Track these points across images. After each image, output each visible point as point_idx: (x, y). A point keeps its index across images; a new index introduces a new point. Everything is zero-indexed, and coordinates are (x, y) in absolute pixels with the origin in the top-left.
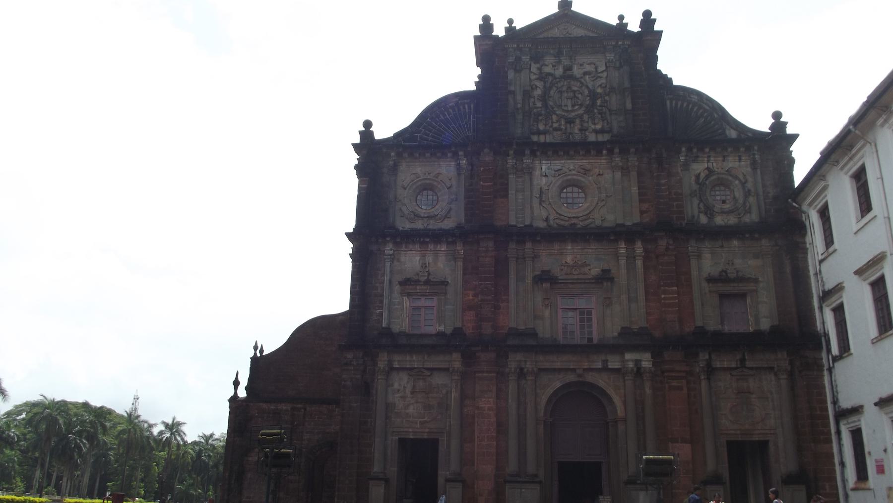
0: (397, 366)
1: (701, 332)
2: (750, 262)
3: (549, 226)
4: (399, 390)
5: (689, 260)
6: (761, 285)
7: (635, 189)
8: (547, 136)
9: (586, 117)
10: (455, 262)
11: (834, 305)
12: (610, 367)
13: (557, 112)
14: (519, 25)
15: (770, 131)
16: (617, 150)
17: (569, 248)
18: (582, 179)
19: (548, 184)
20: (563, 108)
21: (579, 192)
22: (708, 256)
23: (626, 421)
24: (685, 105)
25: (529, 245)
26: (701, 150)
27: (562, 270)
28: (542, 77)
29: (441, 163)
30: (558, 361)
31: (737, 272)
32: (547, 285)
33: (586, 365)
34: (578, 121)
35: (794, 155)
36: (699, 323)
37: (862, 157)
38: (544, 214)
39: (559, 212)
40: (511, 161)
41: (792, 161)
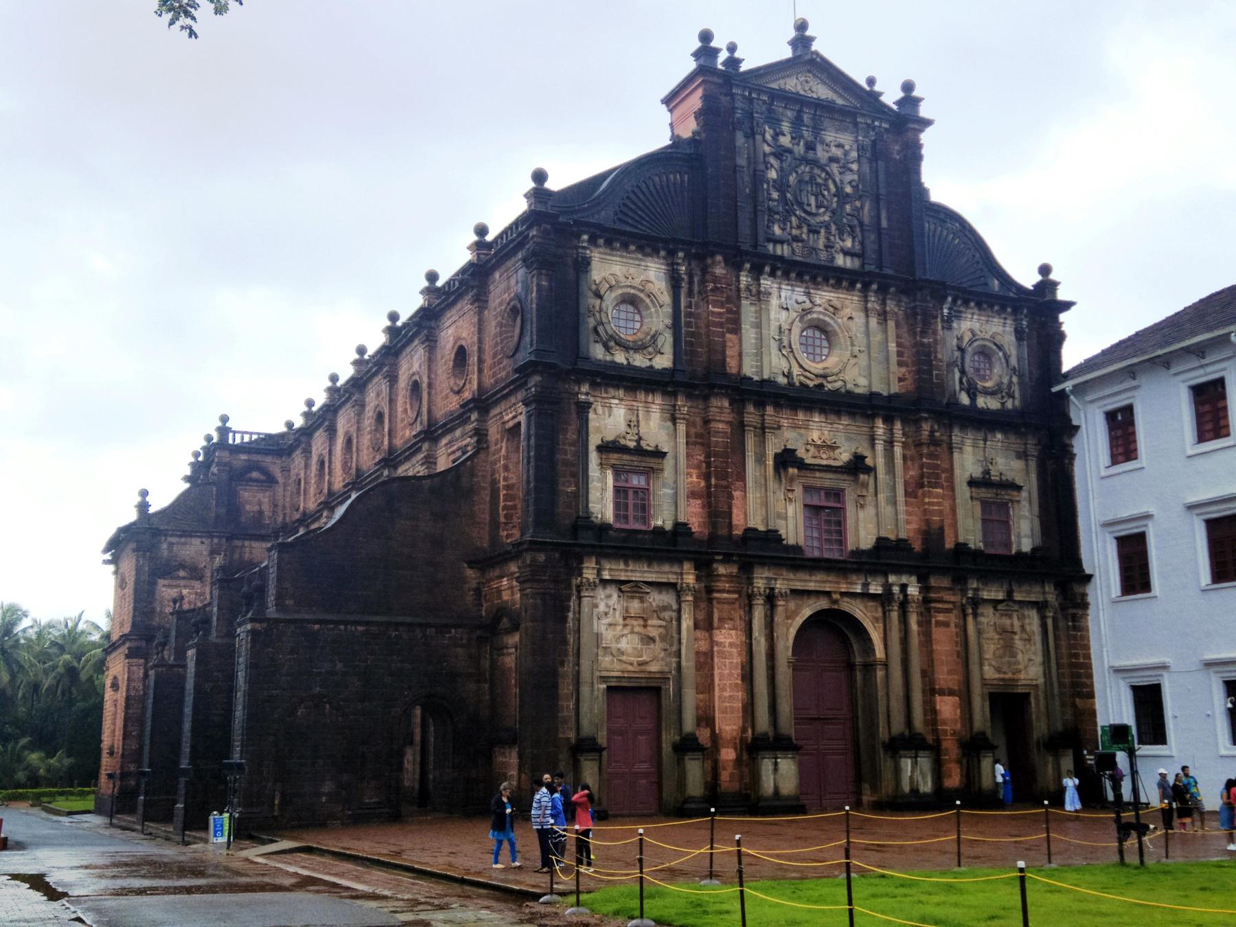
0: (608, 577)
1: (961, 549)
2: (1012, 463)
3: (791, 384)
4: (606, 614)
5: (952, 453)
6: (1024, 494)
7: (893, 347)
8: (785, 247)
9: (833, 228)
10: (675, 424)
11: (1123, 533)
12: (871, 591)
13: (798, 213)
14: (751, 60)
15: (1032, 288)
16: (874, 287)
17: (817, 420)
18: (832, 322)
19: (790, 321)
20: (806, 207)
21: (821, 339)
22: (968, 449)
23: (886, 665)
24: (945, 233)
25: (770, 410)
26: (966, 303)
27: (808, 451)
28: (780, 153)
29: (649, 264)
30: (813, 582)
31: (1001, 474)
32: (793, 471)
33: (844, 588)
34: (823, 231)
35: (1064, 328)
36: (961, 540)
37: (1225, 369)
38: (784, 365)
39: (804, 366)
40: (745, 279)
41: (1061, 337)
